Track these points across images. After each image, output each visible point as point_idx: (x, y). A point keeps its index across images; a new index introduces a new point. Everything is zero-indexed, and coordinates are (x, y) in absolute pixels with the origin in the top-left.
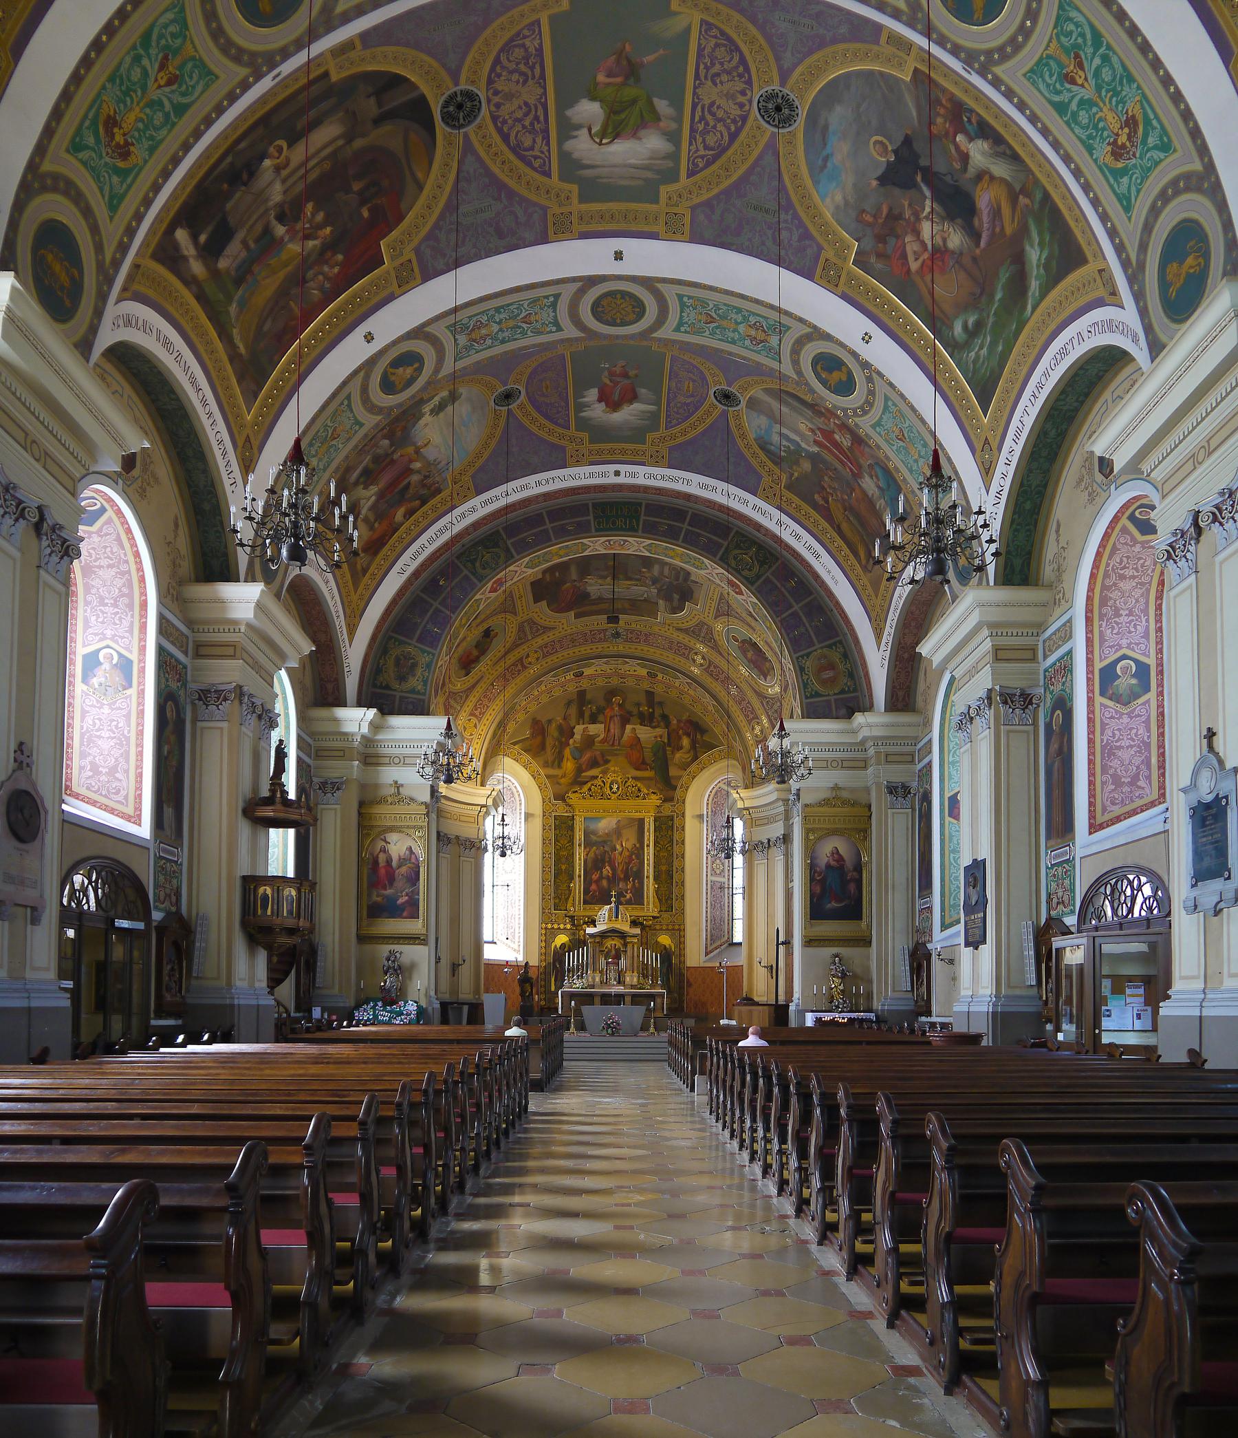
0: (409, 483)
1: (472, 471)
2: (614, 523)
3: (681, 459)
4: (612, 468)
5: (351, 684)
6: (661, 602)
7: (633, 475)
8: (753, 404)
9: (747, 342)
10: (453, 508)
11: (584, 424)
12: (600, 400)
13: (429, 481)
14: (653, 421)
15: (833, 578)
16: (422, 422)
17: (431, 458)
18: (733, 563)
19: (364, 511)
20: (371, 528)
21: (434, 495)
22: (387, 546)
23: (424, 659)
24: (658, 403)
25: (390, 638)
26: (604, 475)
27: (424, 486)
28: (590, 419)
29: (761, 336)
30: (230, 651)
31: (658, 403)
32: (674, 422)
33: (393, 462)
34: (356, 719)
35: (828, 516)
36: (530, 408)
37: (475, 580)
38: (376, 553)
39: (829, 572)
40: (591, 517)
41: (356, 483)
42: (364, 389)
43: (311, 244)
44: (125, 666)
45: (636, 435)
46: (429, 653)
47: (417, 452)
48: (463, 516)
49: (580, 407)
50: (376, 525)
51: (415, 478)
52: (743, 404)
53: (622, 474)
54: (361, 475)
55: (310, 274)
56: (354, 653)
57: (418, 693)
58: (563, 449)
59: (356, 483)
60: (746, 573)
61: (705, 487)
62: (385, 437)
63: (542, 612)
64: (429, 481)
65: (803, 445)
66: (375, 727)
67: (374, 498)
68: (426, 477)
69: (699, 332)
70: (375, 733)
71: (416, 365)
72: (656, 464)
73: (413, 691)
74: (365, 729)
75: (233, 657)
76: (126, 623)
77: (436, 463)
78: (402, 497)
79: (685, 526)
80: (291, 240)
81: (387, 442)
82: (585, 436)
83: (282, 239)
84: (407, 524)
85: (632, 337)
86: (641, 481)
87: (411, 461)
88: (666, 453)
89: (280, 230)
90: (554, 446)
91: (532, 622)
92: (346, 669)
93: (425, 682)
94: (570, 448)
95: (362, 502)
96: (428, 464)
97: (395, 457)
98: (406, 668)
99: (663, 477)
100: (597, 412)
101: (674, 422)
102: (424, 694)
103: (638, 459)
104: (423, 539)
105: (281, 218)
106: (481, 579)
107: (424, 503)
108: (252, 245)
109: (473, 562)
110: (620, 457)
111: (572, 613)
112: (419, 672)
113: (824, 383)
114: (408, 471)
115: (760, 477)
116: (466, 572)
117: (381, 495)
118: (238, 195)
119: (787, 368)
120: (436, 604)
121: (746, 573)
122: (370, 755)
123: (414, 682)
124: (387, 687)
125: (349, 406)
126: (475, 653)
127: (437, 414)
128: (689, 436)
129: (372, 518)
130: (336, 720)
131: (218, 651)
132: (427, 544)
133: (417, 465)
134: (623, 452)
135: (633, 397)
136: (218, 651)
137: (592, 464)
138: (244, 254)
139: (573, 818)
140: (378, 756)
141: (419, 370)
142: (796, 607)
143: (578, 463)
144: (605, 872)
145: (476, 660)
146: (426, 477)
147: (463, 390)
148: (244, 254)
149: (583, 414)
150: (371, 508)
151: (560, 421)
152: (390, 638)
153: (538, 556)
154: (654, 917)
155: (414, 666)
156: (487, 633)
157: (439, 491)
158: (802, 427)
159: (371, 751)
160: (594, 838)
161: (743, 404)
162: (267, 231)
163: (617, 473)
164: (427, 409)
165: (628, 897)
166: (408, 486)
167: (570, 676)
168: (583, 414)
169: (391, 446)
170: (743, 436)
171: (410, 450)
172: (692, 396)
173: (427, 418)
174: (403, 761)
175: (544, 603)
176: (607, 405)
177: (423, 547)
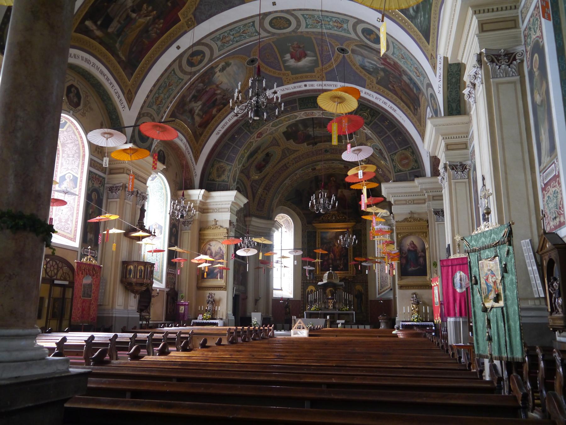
0: (216, 99)
2: (307, 106)
4: (303, 84)
5: (197, 180)
7: (312, 85)
8: (353, 51)
9: (335, 28)
11: (287, 68)
16: (217, 75)
19: (197, 111)
22: (210, 124)
23: (228, 168)
25: (215, 160)
26: (300, 87)
29: (339, 25)
30: (122, 171)
33: (206, 92)
34: (197, 194)
38: (205, 127)
40: (297, 104)
41: (190, 101)
42: (180, 66)
43: (148, 18)
44: (75, 180)
45: (311, 69)
46: (230, 165)
50: (204, 116)
51: (219, 97)
52: (350, 52)
53: (308, 86)
54: (192, 98)
55: (150, 29)
56: (198, 169)
57: (226, 182)
58: (281, 78)
59: (190, 101)
62: (200, 83)
63: (292, 144)
66: (205, 197)
67: (200, 106)
68: (224, 96)
69: (315, 27)
70: (206, 200)
71: (202, 55)
72: (322, 80)
73: (223, 181)
74: (201, 198)
75: (123, 173)
76: (76, 163)
77: (227, 90)
78: (214, 104)
80: (139, 18)
81: (201, 85)
82: (289, 72)
83: (135, 18)
84: (219, 115)
85: (290, 33)
87: (215, 90)
88: (324, 75)
89: (134, 15)
91: (288, 149)
92: (194, 174)
93: (228, 177)
95: (195, 108)
98: (220, 172)
102: (228, 182)
104: (226, 120)
105: (133, 11)
106: (252, 133)
108: (122, 22)
109: (249, 127)
110: (306, 79)
111: (305, 144)
112: (226, 173)
113: (369, 40)
114: (215, 94)
115: (365, 81)
116: (246, 131)
117: (204, 105)
118: (112, 6)
119: (353, 36)
120: (234, 145)
122: (204, 209)
123: (224, 177)
124: (214, 180)
125: (175, 73)
126: (263, 163)
129: (201, 113)
130: (189, 196)
131: (118, 171)
134: (307, 77)
136: (118, 171)
137: (294, 83)
138: (119, 26)
139: (316, 232)
140: (208, 209)
141: (204, 56)
143: (288, 83)
144: (330, 256)
145: (264, 166)
148: (119, 26)
149: (286, 64)
150: (200, 110)
152: (215, 160)
153: (276, 122)
154: (354, 277)
155: (224, 170)
156: (268, 155)
158: (375, 58)
159: (205, 207)
160: (325, 241)
161: (350, 52)
162: (128, 16)
163: (306, 86)
164: (217, 70)
165: (341, 267)
166: (216, 99)
167: (310, 170)
168: (286, 64)
170: (354, 65)
173: (218, 74)
174: (218, 211)
175: (292, 141)
177: (226, 123)
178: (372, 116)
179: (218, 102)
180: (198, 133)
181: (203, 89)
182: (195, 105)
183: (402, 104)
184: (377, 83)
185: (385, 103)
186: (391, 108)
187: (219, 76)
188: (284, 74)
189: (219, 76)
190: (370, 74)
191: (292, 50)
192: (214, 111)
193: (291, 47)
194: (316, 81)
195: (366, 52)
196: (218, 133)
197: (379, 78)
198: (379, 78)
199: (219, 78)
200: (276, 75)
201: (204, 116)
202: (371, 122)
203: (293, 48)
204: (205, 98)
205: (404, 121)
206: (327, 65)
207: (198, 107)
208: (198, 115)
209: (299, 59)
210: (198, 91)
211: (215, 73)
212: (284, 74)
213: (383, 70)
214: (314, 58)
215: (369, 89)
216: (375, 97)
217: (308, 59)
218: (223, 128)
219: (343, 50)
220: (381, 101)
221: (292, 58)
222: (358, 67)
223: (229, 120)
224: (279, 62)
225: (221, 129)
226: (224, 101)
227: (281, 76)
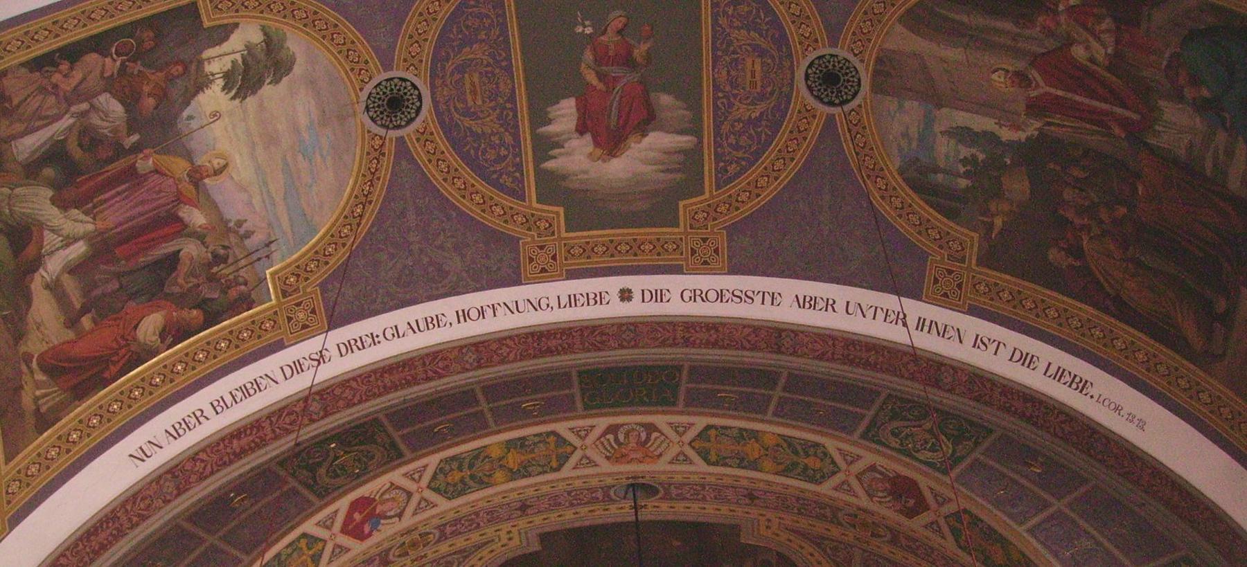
0: (172, 261)
1: (322, 274)
3: (755, 253)
7: (658, 296)
10: (278, 346)
11: (554, 188)
12: (581, 130)
13: (225, 271)
15: (1131, 418)
17: (232, 214)
18: (895, 443)
19: (54, 266)
20: (72, 322)
21: (235, 307)
24: (695, 129)
26: (599, 299)
28: (564, 177)
31: (696, 131)
32: (732, 169)
33: (130, 174)
35: (1086, 286)
36: (442, 144)
37: (312, 497)
38: (80, 392)
39: (1117, 409)
41: (32, 170)
47: (197, 176)
48: (297, 367)
49: (546, 146)
50: (86, 322)
53: (637, 296)
59: (32, 170)
60: (926, 455)
61: (809, 303)
64: (225, 271)
65: (1006, 134)
68: (218, 259)
72: (705, 267)
79: (778, 393)
86: (675, 307)
87: (180, 199)
88: (722, 241)
94: (528, 240)
96: (223, 227)
97: (145, 164)
99: (720, 296)
100: (578, 158)
101: (732, 169)
104: (201, 399)
107: (209, 322)
109: (312, 469)
114: (171, 223)
121: (926, 455)
127: (241, 94)
128: (766, 196)
132: (209, 411)
133: (196, 218)
135: (648, 121)
137: (573, 275)
142: (1057, 505)
143: (544, 275)
146: (218, 259)
147: (296, 44)
149: (549, 165)
150: (74, 269)
151: (507, 181)
157: (247, 302)
166: (172, 261)
168: (549, 165)
169: (133, 125)
171: (179, 167)
172: (762, 97)
173: (213, 98)
176: (597, 144)
177: (199, 417)
178: (957, 441)
179: (181, 281)
180: (27, 400)
181: (120, 151)
182: (52, 214)
183: (1127, 333)
184: (988, 260)
185: (1027, 360)
186: (1060, 375)
187: (216, 115)
188: (530, 222)
189: (216, 115)
190: (952, 214)
191: (592, 78)
192: (150, 326)
193: (588, 56)
194: (677, 270)
195: (954, 54)
196: (141, 456)
197: (998, 222)
198: (998, 222)
199: (218, 129)
200: (493, 221)
201: (86, 322)
202: (955, 460)
203: (602, 58)
204: (118, 213)
205: (1142, 425)
206: (741, 182)
207: (69, 241)
208: (54, 287)
209: (611, 143)
210: (89, 138)
211: (201, 85)
213: (1033, 155)
214: (685, 141)
215: (944, 300)
216: (969, 340)
217: (657, 141)
218: (174, 434)
219: (831, 81)
220: (1005, 353)
221: (581, 130)
222: (896, 180)
223: (219, 406)
224: (517, 144)
225: (162, 439)
226: (209, 292)
227: (513, 229)
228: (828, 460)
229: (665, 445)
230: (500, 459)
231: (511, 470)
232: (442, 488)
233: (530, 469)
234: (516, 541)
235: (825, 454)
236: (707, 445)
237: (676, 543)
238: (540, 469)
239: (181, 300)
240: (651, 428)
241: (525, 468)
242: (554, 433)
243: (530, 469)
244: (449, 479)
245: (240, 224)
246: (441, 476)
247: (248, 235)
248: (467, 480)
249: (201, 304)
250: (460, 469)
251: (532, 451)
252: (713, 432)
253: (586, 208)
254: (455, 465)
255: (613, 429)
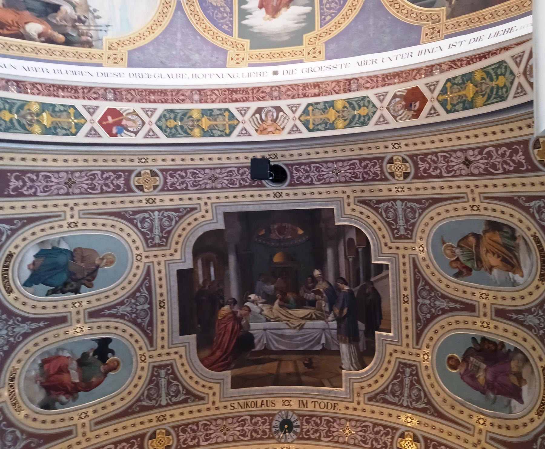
1: (131, 47)
6: (344, 348)
11: (245, 32)
14: (308, 23)
27: (74, 27)
28: (252, 27)
49: (244, 14)
58: (225, 52)
82: (247, 42)
90: (216, 48)
94: (232, 52)
100: (259, 20)
103: (296, 58)
149: (244, 22)
151: (225, 27)
168: (244, 22)
176: (267, 12)
179: (57, 18)
200: (218, 43)
209: (274, 12)
212: (234, 45)
214: (308, 9)
221: (261, 7)
224: (232, 12)
226: (70, 31)
227: (225, 47)
228: (371, 106)
229: (286, 121)
230: (198, 120)
231: (203, 129)
232: (164, 127)
233: (214, 132)
234: (209, 216)
235: (369, 102)
236: (308, 118)
237: (300, 232)
238: (219, 133)
239: (55, 27)
240: (278, 109)
241: (211, 130)
242: (227, 110)
243: (214, 132)
244: (168, 124)
245: (95, 10)
246: (163, 120)
247: (98, 17)
248: (178, 128)
249: (66, 35)
250: (175, 119)
251: (215, 120)
252: (310, 108)
253: (260, 41)
254: (172, 116)
255: (259, 111)
